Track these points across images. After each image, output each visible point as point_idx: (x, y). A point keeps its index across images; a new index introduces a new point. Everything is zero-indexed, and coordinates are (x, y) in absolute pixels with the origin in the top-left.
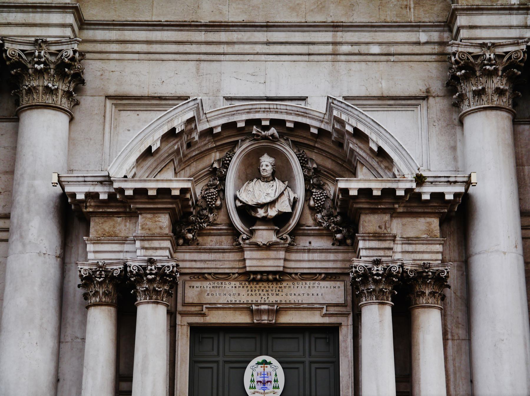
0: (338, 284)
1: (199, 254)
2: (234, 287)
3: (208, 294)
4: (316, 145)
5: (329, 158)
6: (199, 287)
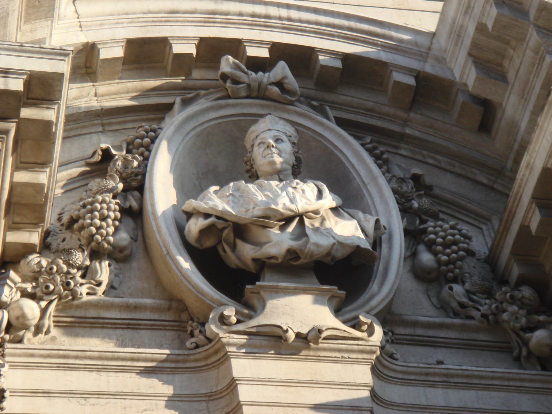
1: (61, 373)
4: (408, 131)
5: (446, 170)
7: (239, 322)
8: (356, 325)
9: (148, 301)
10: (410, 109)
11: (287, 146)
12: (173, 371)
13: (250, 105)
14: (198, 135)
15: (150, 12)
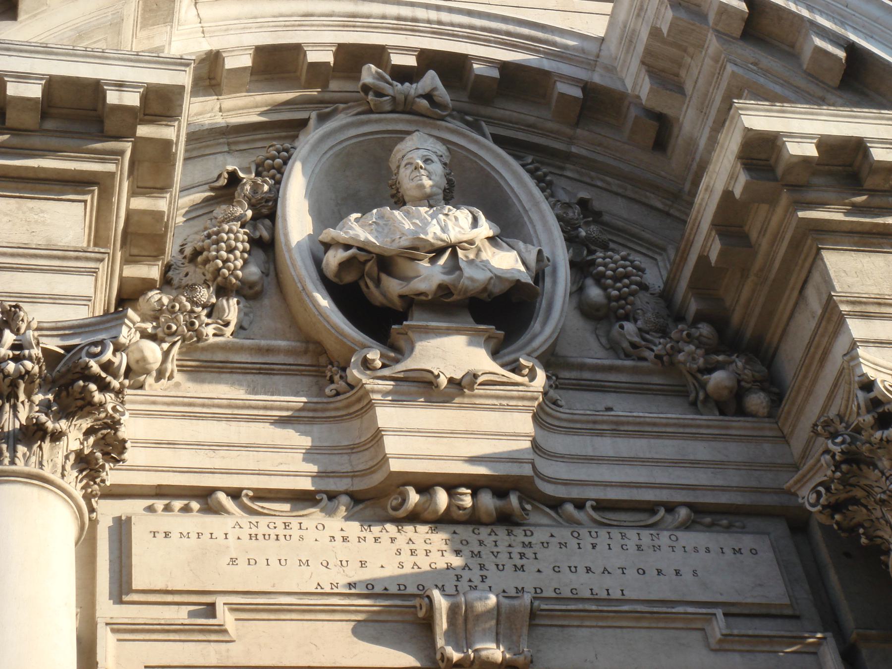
0: (747, 541)
1: (186, 423)
2: (339, 539)
3: (233, 561)
4: (574, 149)
5: (617, 194)
6: (194, 536)
7: (384, 366)
8: (516, 369)
9: (282, 343)
10: (577, 125)
11: (437, 168)
12: (312, 420)
13: (396, 121)
14: (337, 155)
15: (281, 16)
